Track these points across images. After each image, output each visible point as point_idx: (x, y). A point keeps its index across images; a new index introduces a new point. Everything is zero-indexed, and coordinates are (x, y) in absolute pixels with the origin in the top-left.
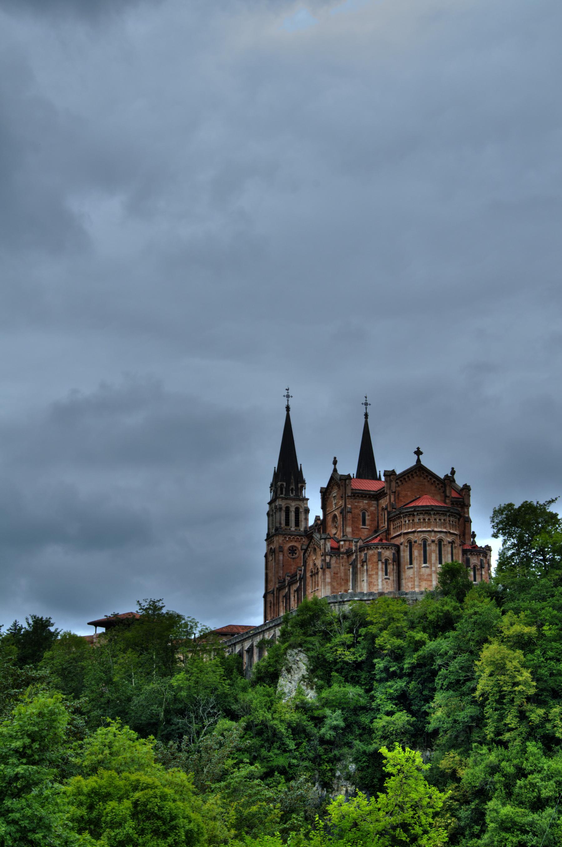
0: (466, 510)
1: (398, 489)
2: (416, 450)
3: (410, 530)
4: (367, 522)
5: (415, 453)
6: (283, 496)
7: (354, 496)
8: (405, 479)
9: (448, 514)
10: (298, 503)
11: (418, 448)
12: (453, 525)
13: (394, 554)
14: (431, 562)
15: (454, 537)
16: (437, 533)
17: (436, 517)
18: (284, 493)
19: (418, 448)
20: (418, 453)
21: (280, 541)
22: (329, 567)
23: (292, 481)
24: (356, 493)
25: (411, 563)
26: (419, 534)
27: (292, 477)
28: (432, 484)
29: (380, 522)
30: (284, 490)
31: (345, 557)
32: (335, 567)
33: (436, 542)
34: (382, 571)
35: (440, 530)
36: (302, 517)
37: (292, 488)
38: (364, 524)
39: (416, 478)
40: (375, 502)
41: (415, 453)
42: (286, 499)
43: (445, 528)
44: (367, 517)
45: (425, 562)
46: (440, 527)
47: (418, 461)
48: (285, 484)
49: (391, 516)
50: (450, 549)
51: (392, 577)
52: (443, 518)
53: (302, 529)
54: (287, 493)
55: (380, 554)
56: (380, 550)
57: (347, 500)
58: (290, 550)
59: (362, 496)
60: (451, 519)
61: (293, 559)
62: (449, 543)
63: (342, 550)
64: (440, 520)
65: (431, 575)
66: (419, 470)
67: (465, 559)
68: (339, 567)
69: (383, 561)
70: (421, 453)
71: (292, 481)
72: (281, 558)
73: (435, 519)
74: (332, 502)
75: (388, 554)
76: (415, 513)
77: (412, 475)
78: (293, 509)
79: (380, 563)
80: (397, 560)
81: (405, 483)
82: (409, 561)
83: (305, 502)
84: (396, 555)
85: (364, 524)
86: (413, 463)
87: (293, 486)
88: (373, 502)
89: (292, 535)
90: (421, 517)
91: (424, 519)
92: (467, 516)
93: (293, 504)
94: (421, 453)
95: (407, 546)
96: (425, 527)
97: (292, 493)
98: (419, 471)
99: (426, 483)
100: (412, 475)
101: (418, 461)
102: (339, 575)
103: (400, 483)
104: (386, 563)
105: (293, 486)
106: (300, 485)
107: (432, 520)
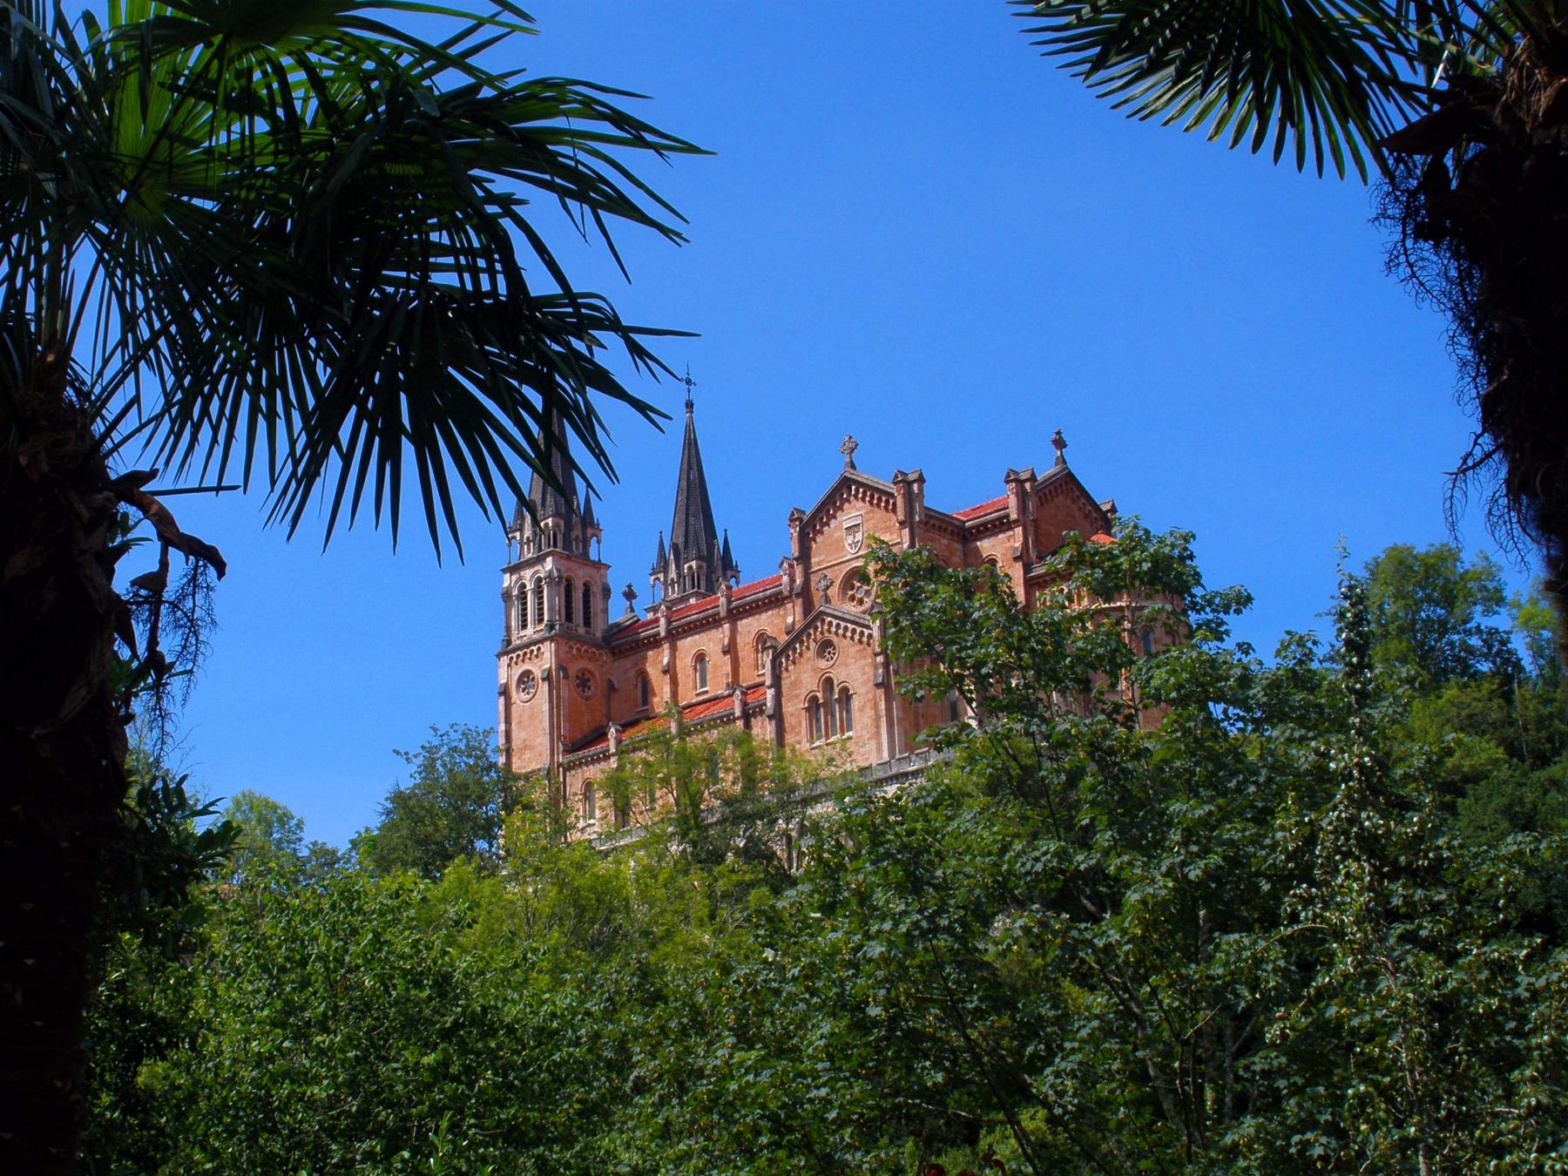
10: (589, 571)
18: (560, 544)
20: (1060, 443)
21: (562, 655)
30: (559, 537)
36: (596, 603)
42: (568, 558)
53: (599, 634)
54: (567, 546)
57: (917, 531)
61: (587, 699)
66: (1067, 483)
74: (840, 540)
89: (583, 643)
93: (581, 573)
99: (1077, 514)
105: (577, 532)
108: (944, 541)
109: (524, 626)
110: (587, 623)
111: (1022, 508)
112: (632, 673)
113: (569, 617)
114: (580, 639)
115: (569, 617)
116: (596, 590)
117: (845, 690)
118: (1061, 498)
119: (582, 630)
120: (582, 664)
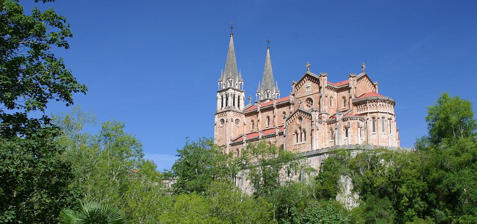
10: (240, 93)
22: (318, 130)
25: (374, 131)
26: (380, 114)
29: (339, 106)
31: (326, 124)
36: (242, 102)
38: (331, 106)
40: (336, 93)
44: (332, 102)
45: (383, 131)
55: (358, 123)
63: (324, 119)
72: (232, 125)
75: (362, 124)
78: (237, 96)
80: (366, 128)
82: (372, 129)
90: (381, 103)
102: (321, 135)
107: (387, 106)
108: (332, 92)
109: (222, 107)
110: (239, 107)
112: (250, 120)
113: (234, 105)
115: (234, 105)
117: (304, 130)
119: (237, 108)
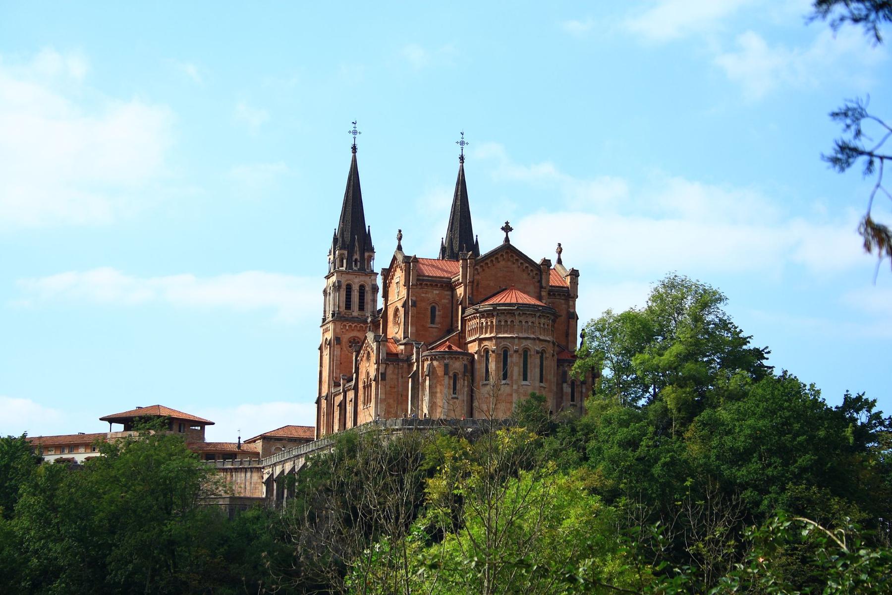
0: (571, 303)
1: (477, 277)
2: (504, 225)
3: (488, 335)
4: (437, 319)
5: (503, 229)
6: (344, 269)
7: (421, 284)
8: (487, 264)
9: (538, 314)
11: (507, 223)
12: (544, 329)
13: (465, 366)
14: (512, 377)
15: (545, 345)
16: (523, 341)
17: (521, 318)
18: (345, 265)
19: (507, 223)
20: (507, 229)
21: (338, 330)
23: (357, 248)
24: (423, 280)
27: (357, 244)
28: (524, 270)
30: (345, 261)
32: (392, 379)
33: (521, 351)
34: (449, 388)
35: (526, 335)
36: (368, 297)
37: (356, 260)
38: (433, 322)
39: (502, 263)
40: (449, 293)
41: (503, 229)
43: (533, 333)
46: (526, 331)
47: (507, 239)
48: (346, 252)
49: (465, 315)
50: (538, 361)
51: (463, 396)
52: (530, 319)
54: (349, 266)
56: (446, 361)
58: (350, 342)
59: (431, 285)
60: (543, 321)
62: (538, 352)
64: (527, 322)
65: (511, 395)
67: (560, 371)
68: (398, 379)
69: (451, 374)
70: (511, 229)
71: (357, 248)
73: (520, 322)
76: (495, 313)
77: (497, 258)
79: (446, 377)
81: (487, 269)
83: (373, 277)
84: (469, 367)
85: (433, 322)
86: (500, 242)
87: (357, 256)
88: (446, 293)
89: (354, 322)
90: (502, 318)
91: (506, 321)
92: (572, 310)
93: (356, 280)
94: (511, 229)
95: (482, 356)
96: (506, 332)
97: (356, 265)
98: (507, 253)
99: (516, 270)
100: (497, 258)
101: (507, 239)
103: (480, 270)
104: (455, 378)
105: (357, 256)
106: (366, 254)
107: (516, 323)
110: (362, 308)
111: (464, 276)
113: (348, 306)
114: (353, 319)
115: (348, 306)
116: (368, 288)
118: (502, 263)
119: (356, 313)
120: (355, 334)
